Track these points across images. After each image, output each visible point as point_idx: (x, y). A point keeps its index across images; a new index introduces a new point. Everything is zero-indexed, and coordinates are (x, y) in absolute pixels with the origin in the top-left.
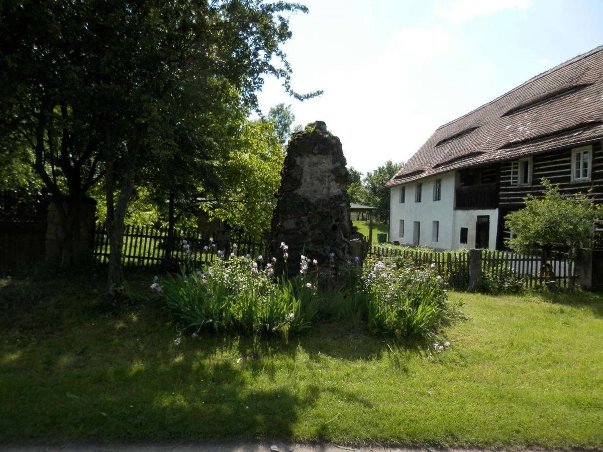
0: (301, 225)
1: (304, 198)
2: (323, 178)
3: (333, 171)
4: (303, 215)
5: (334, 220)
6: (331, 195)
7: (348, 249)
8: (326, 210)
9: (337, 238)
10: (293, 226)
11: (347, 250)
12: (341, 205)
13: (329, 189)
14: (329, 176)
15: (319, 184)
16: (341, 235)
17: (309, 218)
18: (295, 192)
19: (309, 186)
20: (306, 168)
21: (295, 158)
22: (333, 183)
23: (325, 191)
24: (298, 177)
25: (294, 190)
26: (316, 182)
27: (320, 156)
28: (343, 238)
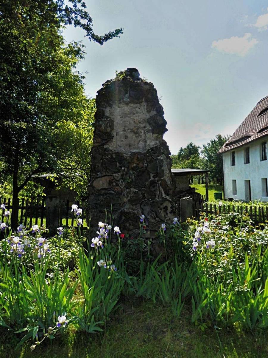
0: (114, 184)
1: (115, 153)
2: (138, 129)
3: (148, 121)
4: (115, 172)
5: (152, 175)
6: (148, 148)
7: (171, 208)
8: (141, 165)
9: (157, 196)
10: (106, 186)
11: (169, 209)
12: (159, 158)
13: (146, 142)
14: (145, 127)
15: (134, 137)
16: (161, 192)
17: (122, 175)
18: (105, 147)
19: (122, 139)
20: (117, 120)
21: (104, 109)
22: (149, 135)
23: (141, 144)
24: (109, 130)
25: (103, 144)
26: (130, 135)
27: (132, 105)
28: (164, 195)
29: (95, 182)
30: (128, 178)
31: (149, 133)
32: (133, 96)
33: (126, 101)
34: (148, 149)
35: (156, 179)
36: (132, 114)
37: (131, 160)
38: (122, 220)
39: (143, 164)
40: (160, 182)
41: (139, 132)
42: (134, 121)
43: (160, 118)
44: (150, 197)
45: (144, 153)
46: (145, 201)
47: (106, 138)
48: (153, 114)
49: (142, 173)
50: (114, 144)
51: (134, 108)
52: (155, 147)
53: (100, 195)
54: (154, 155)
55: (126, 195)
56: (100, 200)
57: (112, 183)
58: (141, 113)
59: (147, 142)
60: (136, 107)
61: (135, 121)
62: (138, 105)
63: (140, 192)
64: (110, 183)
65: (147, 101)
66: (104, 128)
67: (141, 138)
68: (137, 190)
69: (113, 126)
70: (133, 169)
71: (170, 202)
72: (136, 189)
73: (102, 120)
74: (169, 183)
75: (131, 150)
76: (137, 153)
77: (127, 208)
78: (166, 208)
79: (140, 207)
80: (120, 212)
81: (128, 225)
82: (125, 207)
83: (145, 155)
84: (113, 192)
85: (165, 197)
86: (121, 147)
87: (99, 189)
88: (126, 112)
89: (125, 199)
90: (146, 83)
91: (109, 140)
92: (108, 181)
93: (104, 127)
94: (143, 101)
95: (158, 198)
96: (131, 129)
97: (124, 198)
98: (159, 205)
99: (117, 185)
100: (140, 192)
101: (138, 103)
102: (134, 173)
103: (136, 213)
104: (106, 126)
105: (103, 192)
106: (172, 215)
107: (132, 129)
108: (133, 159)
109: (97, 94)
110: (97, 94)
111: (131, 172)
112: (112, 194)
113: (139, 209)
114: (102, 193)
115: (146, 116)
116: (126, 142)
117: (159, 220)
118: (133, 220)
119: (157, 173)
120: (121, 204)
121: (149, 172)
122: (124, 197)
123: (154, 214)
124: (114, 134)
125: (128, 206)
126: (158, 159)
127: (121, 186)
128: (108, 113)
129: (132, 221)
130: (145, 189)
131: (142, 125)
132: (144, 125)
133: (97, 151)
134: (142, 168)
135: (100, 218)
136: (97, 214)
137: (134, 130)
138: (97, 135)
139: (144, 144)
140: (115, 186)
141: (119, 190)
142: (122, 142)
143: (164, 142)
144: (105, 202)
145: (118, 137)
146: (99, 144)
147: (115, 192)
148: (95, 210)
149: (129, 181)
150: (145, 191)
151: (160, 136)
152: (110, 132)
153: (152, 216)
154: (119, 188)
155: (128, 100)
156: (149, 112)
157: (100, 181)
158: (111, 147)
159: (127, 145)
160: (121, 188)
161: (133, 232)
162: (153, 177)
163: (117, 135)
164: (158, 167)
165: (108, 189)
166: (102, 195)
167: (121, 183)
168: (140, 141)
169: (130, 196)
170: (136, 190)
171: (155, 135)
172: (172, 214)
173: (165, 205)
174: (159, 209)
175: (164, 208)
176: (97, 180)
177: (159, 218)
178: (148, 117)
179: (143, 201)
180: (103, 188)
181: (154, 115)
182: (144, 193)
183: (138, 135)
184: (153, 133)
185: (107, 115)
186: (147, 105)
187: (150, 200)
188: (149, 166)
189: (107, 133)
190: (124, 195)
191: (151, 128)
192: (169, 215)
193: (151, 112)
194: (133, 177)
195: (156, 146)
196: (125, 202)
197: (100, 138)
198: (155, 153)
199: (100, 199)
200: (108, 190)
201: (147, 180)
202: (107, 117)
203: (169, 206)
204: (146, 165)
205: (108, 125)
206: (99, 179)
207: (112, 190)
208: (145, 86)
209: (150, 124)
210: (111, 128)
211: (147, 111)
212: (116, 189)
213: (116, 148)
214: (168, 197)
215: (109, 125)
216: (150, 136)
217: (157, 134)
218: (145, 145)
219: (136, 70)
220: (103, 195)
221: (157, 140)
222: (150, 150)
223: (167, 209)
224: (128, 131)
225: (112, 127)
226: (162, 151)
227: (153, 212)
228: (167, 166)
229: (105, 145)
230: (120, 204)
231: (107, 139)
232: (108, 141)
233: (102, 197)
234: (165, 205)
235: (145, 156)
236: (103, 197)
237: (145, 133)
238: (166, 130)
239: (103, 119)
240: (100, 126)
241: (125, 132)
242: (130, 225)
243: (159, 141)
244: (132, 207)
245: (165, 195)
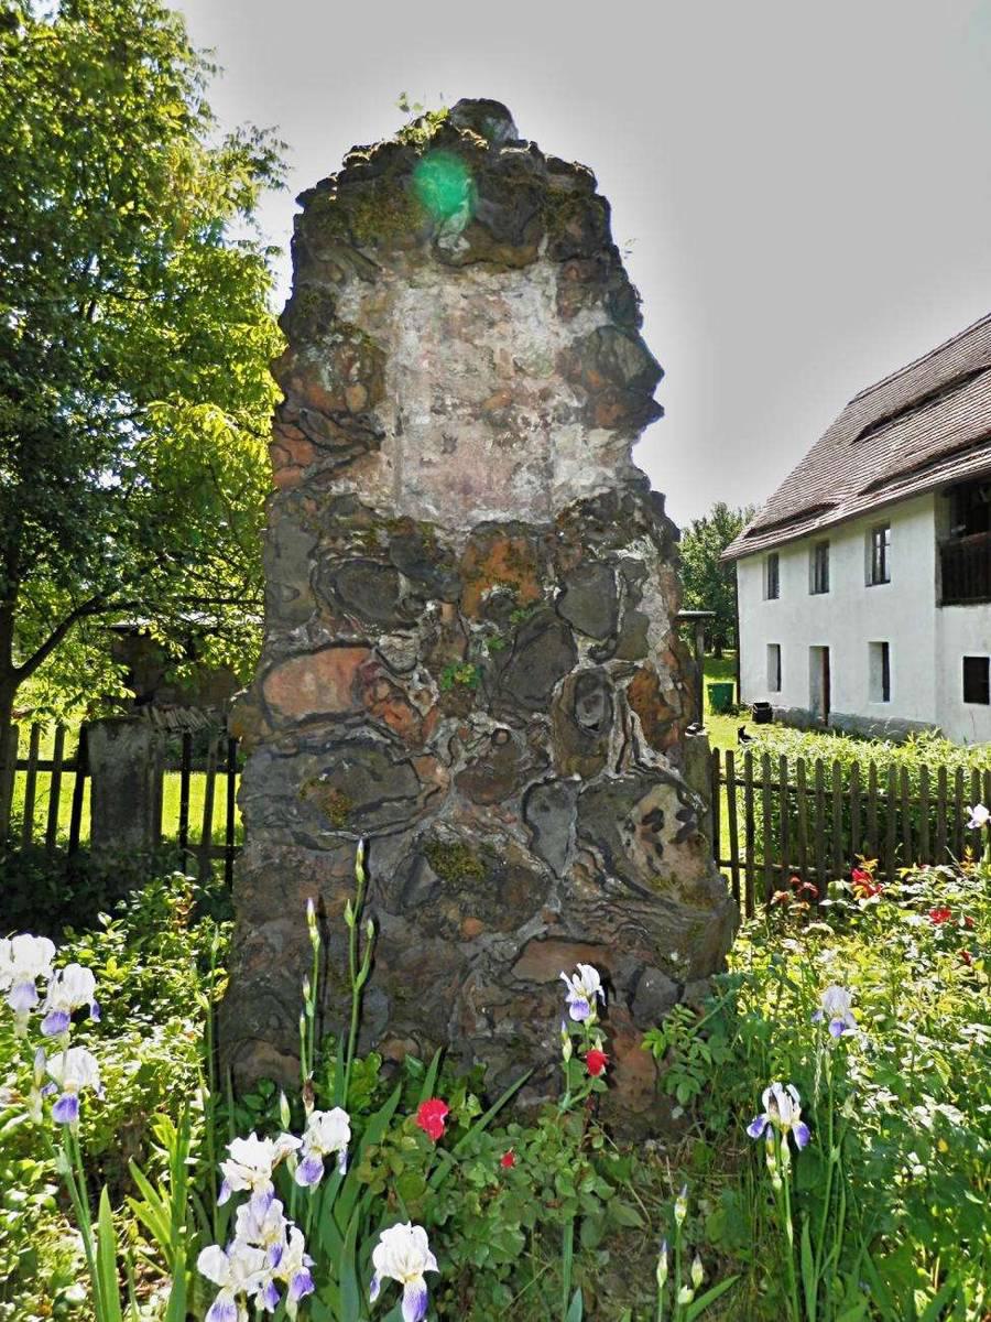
0: (383, 690)
1: (392, 524)
2: (509, 405)
3: (566, 367)
4: (387, 628)
5: (584, 645)
6: (562, 501)
7: (680, 816)
8: (527, 590)
9: (613, 758)
10: (335, 700)
11: (671, 826)
12: (622, 553)
13: (549, 472)
14: (545, 395)
15: (489, 444)
16: (631, 739)
17: (428, 643)
18: (338, 488)
19: (427, 456)
20: (412, 346)
21: (332, 288)
22: (569, 436)
23: (525, 485)
24: (357, 397)
25: (329, 475)
26: (473, 434)
27: (483, 277)
28: (646, 754)
29: (274, 678)
30: (460, 659)
31: (566, 427)
32: (490, 222)
33: (450, 251)
34: (561, 506)
35: (606, 666)
36: (480, 324)
37: (476, 563)
38: (423, 884)
39: (540, 582)
40: (626, 682)
41: (515, 419)
42: (491, 361)
43: (630, 345)
44: (574, 762)
45: (546, 527)
46: (548, 782)
47: (341, 442)
48: (593, 327)
49: (535, 635)
50: (382, 474)
51: (494, 292)
52: (601, 496)
53: (303, 748)
54: (597, 537)
55: (444, 751)
56: (306, 780)
57: (371, 683)
58: (534, 320)
59: (557, 471)
60: (503, 288)
61: (497, 359)
62: (515, 276)
63: (519, 737)
64: (363, 683)
65: (561, 255)
66: (329, 388)
67: (524, 453)
68: (505, 727)
69: (383, 381)
70: (488, 610)
71: (678, 787)
72: (500, 720)
73: (318, 345)
74: (671, 686)
75: (474, 512)
76: (506, 525)
77: (449, 820)
78: (655, 819)
79: (518, 815)
80: (413, 845)
81: (453, 915)
82: (441, 815)
83: (548, 535)
84: (375, 736)
85: (650, 764)
86: (419, 494)
87: (301, 717)
88: (449, 311)
89: (440, 770)
90: (557, 166)
91: (359, 449)
92: (349, 677)
93: (332, 380)
94: (541, 252)
95: (618, 771)
96: (473, 405)
97: (435, 766)
98: (623, 805)
99: (400, 695)
100: (519, 737)
101: (513, 267)
102: (489, 633)
103: (500, 849)
104: (342, 381)
105: (321, 732)
106: (687, 853)
107: (482, 403)
108: (487, 555)
109: (300, 210)
110: (300, 210)
111: (476, 628)
112: (371, 745)
113: (514, 828)
114: (316, 741)
115: (553, 338)
116: (443, 468)
117: (624, 889)
118: (483, 888)
119: (614, 635)
120: (420, 800)
121: (571, 626)
122: (433, 760)
123: (599, 856)
124: (388, 425)
125: (452, 807)
126: (617, 561)
127: (416, 703)
128: (355, 307)
129: (477, 892)
130: (545, 718)
131: (531, 385)
132: (542, 384)
133: (291, 506)
134: (531, 606)
135: (299, 876)
136: (283, 857)
137: (487, 407)
138: (295, 423)
139: (538, 483)
140: (386, 700)
141: (405, 721)
142: (425, 471)
143: (639, 477)
144: (332, 791)
145: (404, 440)
146: (302, 473)
147: (384, 732)
148: (276, 834)
149: (466, 674)
150: (548, 728)
151: (622, 442)
152: (363, 410)
153: (585, 869)
154: (410, 712)
155: (464, 244)
156: (566, 314)
157: (302, 673)
158: (371, 491)
159: (451, 486)
160: (417, 711)
161: (479, 949)
162: (592, 654)
163: (399, 432)
164: (617, 601)
165: (345, 716)
166: (314, 750)
167: (420, 686)
168: (519, 465)
169: (464, 755)
170: (499, 725)
171: (600, 436)
172: (684, 845)
173: (648, 803)
174: (620, 826)
175: (645, 821)
176: (285, 668)
177: (625, 880)
178: (565, 339)
179: (537, 785)
180: (323, 711)
181: (598, 330)
182: (545, 743)
183: (507, 434)
184: (590, 425)
185: (351, 319)
186: (562, 278)
187: (577, 778)
188: (570, 598)
189: (346, 413)
190: (434, 753)
191: (579, 397)
192: (670, 854)
193: (583, 313)
194: (485, 654)
195: (606, 490)
196: (438, 790)
197: (309, 439)
198: (600, 530)
199: (301, 772)
200: (349, 721)
201: (559, 671)
202: (348, 330)
203: (670, 804)
204: (557, 590)
205: (354, 371)
206: (297, 661)
207: (367, 722)
208: (549, 176)
209: (572, 379)
210: (368, 390)
211: (561, 312)
212: (390, 720)
213: (397, 496)
214: (663, 762)
215: (360, 370)
216: (574, 439)
217: (607, 428)
218: (547, 488)
219: (499, 111)
220: (319, 751)
221: (605, 464)
222: (575, 515)
223: (661, 826)
224: (460, 412)
225: (374, 381)
226: (637, 516)
227: (592, 843)
228: (659, 598)
229: (336, 478)
230: (412, 800)
231: (344, 449)
232: (354, 458)
233: (312, 759)
234: (648, 803)
235: (547, 540)
236: (321, 761)
237: (546, 425)
238: (656, 412)
239: (327, 339)
240: (309, 372)
241: (442, 419)
242: (464, 912)
243: (618, 471)
244: (476, 811)
245: (652, 754)
